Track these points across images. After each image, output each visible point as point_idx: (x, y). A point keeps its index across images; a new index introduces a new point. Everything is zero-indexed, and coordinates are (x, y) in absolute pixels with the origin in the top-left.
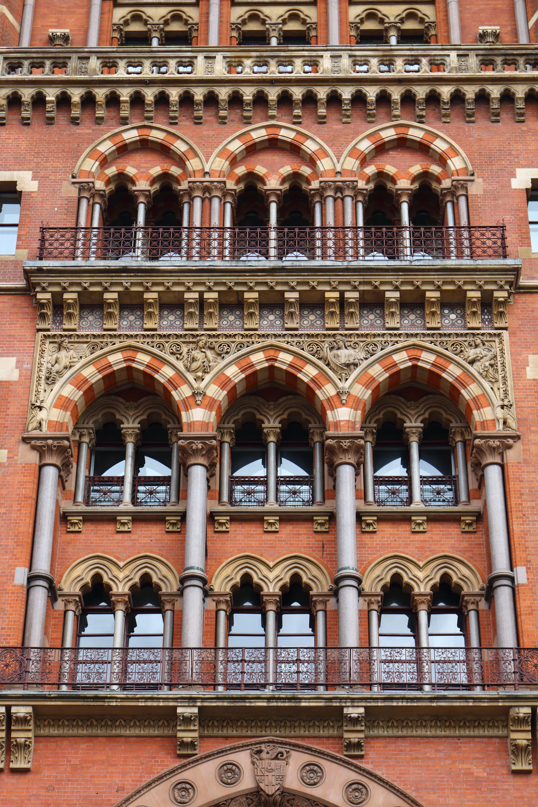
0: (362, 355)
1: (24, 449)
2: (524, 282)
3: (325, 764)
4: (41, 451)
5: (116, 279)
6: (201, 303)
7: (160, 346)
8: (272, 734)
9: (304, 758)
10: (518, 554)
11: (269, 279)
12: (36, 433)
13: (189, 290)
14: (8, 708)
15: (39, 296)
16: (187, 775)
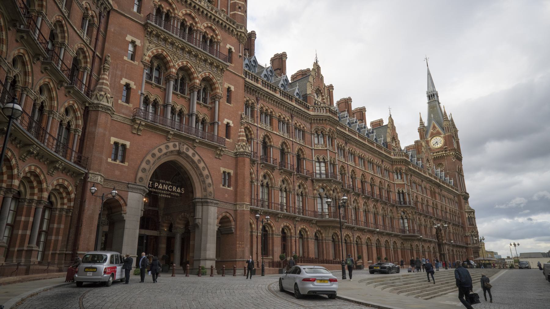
1: (141, 63)
3: (190, 149)
4: (145, 66)
5: (164, 33)
8: (183, 140)
11: (191, 48)
13: (177, 43)
14: (141, 122)
15: (148, 29)
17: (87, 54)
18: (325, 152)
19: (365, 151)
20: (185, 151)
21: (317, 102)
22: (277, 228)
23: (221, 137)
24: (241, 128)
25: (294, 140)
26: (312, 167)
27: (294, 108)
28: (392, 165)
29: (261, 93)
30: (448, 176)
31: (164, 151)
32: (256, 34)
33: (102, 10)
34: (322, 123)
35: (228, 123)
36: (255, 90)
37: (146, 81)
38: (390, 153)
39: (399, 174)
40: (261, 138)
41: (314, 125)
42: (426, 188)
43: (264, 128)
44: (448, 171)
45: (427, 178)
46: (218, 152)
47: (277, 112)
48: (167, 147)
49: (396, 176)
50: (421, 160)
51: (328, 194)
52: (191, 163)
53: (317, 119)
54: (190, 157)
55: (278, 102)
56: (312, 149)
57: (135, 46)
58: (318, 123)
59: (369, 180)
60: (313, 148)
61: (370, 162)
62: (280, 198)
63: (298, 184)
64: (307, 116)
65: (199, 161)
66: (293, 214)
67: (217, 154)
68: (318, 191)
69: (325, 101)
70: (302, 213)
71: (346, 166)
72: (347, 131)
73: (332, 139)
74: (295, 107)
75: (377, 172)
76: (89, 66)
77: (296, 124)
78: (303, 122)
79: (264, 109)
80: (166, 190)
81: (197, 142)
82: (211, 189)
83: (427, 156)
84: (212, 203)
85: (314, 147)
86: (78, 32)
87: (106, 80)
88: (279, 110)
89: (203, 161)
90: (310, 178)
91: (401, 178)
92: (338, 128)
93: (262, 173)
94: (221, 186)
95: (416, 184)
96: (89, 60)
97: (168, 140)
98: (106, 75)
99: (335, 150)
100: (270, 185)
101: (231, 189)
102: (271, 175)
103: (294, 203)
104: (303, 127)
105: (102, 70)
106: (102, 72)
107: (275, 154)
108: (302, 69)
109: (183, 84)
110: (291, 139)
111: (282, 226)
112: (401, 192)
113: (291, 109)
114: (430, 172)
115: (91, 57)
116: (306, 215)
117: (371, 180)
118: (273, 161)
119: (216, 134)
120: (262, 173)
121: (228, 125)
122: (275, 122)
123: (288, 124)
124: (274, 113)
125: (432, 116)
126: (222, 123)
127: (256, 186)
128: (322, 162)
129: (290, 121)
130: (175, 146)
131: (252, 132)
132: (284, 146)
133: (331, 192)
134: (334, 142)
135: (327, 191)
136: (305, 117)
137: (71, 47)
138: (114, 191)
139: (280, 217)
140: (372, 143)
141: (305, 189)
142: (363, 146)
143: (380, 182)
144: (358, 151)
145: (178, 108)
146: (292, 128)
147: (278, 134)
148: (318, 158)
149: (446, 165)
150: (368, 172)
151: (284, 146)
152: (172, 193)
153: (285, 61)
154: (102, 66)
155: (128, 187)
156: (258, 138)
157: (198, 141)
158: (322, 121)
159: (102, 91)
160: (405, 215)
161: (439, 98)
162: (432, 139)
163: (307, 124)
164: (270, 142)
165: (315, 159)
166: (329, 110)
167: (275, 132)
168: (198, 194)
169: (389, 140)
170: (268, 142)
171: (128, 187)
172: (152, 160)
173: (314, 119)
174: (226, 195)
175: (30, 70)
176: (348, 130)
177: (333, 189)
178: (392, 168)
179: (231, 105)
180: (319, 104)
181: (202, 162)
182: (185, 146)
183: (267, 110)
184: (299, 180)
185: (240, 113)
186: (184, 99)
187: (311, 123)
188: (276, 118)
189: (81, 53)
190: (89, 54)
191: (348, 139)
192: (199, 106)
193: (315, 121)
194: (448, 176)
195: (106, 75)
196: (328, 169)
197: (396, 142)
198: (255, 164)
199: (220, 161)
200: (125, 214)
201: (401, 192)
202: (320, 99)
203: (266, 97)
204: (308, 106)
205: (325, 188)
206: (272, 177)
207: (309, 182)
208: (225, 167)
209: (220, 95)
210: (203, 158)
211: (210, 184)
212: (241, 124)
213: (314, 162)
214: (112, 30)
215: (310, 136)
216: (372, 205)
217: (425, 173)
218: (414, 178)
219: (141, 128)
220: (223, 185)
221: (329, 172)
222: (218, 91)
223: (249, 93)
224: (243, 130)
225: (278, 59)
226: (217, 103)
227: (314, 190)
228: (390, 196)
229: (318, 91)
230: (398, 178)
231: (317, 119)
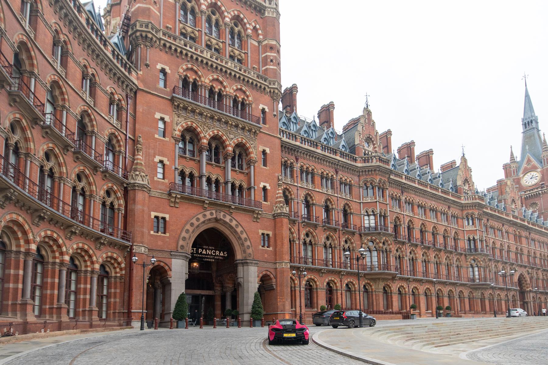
0: (233, 137)
1: (172, 139)
2: (261, 130)
3: (227, 215)
4: (176, 141)
6: (206, 116)
7: (198, 123)
8: (219, 208)
9: (224, 213)
10: (256, 184)
12: (175, 136)
16: (205, 213)
17: (119, 138)
18: (375, 204)
19: (426, 198)
20: (222, 217)
21: (367, 152)
22: (321, 283)
23: (259, 200)
24: (279, 190)
26: (360, 221)
27: (339, 162)
28: (462, 210)
29: (300, 151)
30: (542, 216)
31: (202, 219)
32: (297, 88)
33: (129, 92)
34: (372, 174)
35: (265, 187)
36: (294, 149)
37: (178, 155)
38: (459, 198)
39: (470, 219)
41: (362, 177)
42: (508, 233)
43: (305, 187)
44: (543, 211)
45: (510, 221)
46: (256, 216)
47: (319, 169)
48: (205, 216)
49: (466, 222)
50: (503, 201)
51: (377, 246)
52: (230, 228)
53: (365, 171)
54: (228, 223)
55: (320, 158)
56: (360, 203)
57: (165, 123)
58: (366, 175)
59: (430, 228)
61: (432, 210)
62: (321, 254)
63: (344, 239)
64: (355, 169)
65: (237, 225)
66: (338, 269)
67: (254, 218)
68: (367, 245)
69: (376, 149)
70: (350, 267)
71: (401, 217)
72: (404, 179)
73: (383, 190)
74: (339, 161)
75: (442, 220)
76: (123, 149)
77: (341, 178)
78: (350, 176)
79: (305, 167)
80: (210, 255)
81: (233, 209)
82: (250, 251)
83: (513, 196)
84: (251, 263)
85: (363, 200)
86: (106, 118)
87: (140, 159)
88: (322, 166)
89: (241, 225)
91: (473, 224)
92: (391, 177)
93: (304, 232)
94: (261, 247)
95: (494, 229)
96: (122, 143)
97: (205, 209)
98: (140, 155)
99: (387, 202)
100: (313, 243)
101: (271, 249)
102: (314, 233)
103: (340, 258)
104: (350, 181)
105: (136, 151)
106: (136, 153)
108: (354, 118)
109: (217, 154)
110: (336, 195)
111: (327, 280)
112: (472, 239)
113: (335, 164)
114: (516, 214)
115: (124, 141)
116: (353, 269)
117: (433, 229)
118: (316, 218)
119: (253, 199)
120: (303, 232)
121: (264, 189)
122: (317, 179)
123: (332, 180)
124: (315, 170)
125: (527, 147)
126: (258, 187)
127: (298, 245)
128: (371, 215)
129: (335, 176)
130: (212, 214)
131: (292, 193)
132: (328, 203)
133: (381, 245)
134: (386, 193)
135: (376, 244)
136: (352, 170)
137: (101, 133)
138: (153, 259)
139: (324, 273)
140: (436, 189)
141: (352, 243)
142: (424, 193)
143: (445, 230)
144: (417, 199)
145: (214, 178)
146: (337, 184)
147: (321, 191)
149: (541, 204)
150: (430, 220)
152: (215, 257)
153: (332, 112)
154: (136, 147)
155: (171, 255)
156: (299, 197)
157: (233, 207)
158: (372, 172)
159: (137, 171)
160: (475, 263)
161: (539, 124)
162: (525, 175)
163: (355, 177)
164: (313, 200)
165: (364, 212)
166: (380, 159)
167: (318, 190)
168: (239, 256)
169: (459, 183)
170: (310, 200)
171: (172, 254)
172: (191, 229)
173: (362, 171)
174: (266, 255)
175: (62, 161)
176: (405, 178)
177: (382, 241)
178: (462, 214)
179: (267, 168)
180: (370, 153)
181: (240, 227)
182: (222, 213)
183: (307, 168)
184: (346, 235)
185: (277, 175)
186: (219, 169)
187: (359, 176)
188: (319, 175)
189: (114, 138)
190: (121, 137)
191: (404, 188)
192: (235, 173)
193: (364, 173)
194: (542, 216)
195: (140, 155)
196: (377, 221)
197: (469, 184)
198: (295, 224)
199: (258, 223)
200: (171, 277)
201: (472, 239)
202: (371, 149)
203: (307, 155)
204: (356, 157)
205: (374, 242)
206: (315, 234)
207: (357, 236)
208: (263, 229)
209: (254, 159)
210: (241, 223)
211: (249, 246)
212: (279, 186)
213: (362, 216)
214: (141, 110)
215: (358, 189)
216: (434, 255)
217: (507, 215)
218: (492, 223)
219: (178, 201)
220: (263, 246)
221: (379, 224)
222: (252, 155)
223: (287, 153)
224: (281, 191)
225: (324, 111)
226: (252, 167)
228: (458, 244)
229: (369, 140)
230: (468, 224)
231: (365, 171)
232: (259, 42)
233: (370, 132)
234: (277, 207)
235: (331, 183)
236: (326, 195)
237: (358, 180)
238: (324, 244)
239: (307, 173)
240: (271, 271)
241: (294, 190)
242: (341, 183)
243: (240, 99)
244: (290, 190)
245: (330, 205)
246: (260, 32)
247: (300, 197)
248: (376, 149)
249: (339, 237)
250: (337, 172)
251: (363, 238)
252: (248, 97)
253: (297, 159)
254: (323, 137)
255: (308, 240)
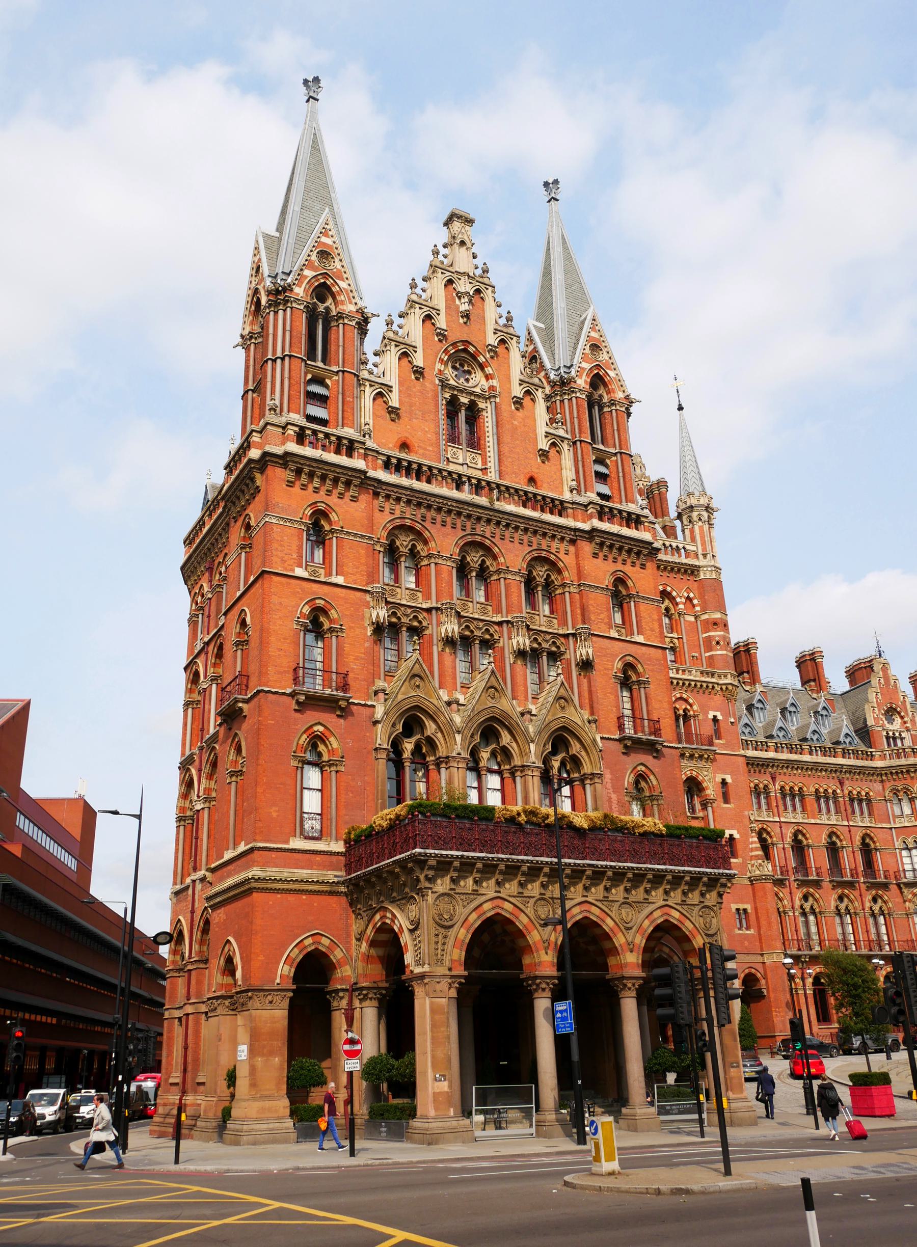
25: (851, 823)
40: (789, 839)
55: (810, 767)
56: (891, 828)
60: (893, 825)
77: (850, 792)
85: (895, 822)
90: (895, 882)
94: (737, 932)
100: (817, 910)
102: (817, 895)
107: (818, 859)
122: (811, 801)
124: (805, 789)
129: (838, 791)
147: (819, 822)
148: (904, 842)
151: (834, 838)
163: (875, 785)
165: (900, 844)
174: (746, 942)
183: (792, 788)
187: (882, 781)
188: (811, 795)
204: (871, 752)
220: (740, 929)
227: (905, 901)
232: (696, 617)
233: (891, 699)
234: (753, 866)
235: (835, 802)
236: (828, 827)
237: (881, 788)
238: (835, 910)
239: (793, 796)
240: (756, 968)
241: (775, 830)
242: (852, 800)
243: (681, 712)
244: (769, 829)
245: (838, 841)
246: (695, 602)
247: (786, 838)
248: (908, 725)
249: (861, 895)
250: (841, 784)
251: (905, 891)
252: (691, 705)
253: (774, 779)
254: (810, 730)
255: (807, 906)
